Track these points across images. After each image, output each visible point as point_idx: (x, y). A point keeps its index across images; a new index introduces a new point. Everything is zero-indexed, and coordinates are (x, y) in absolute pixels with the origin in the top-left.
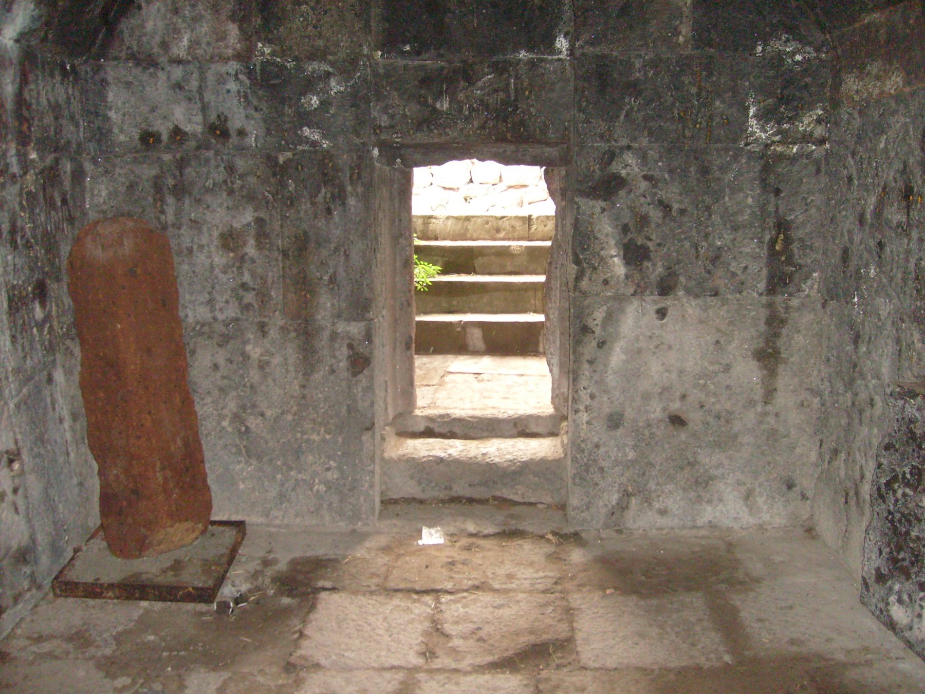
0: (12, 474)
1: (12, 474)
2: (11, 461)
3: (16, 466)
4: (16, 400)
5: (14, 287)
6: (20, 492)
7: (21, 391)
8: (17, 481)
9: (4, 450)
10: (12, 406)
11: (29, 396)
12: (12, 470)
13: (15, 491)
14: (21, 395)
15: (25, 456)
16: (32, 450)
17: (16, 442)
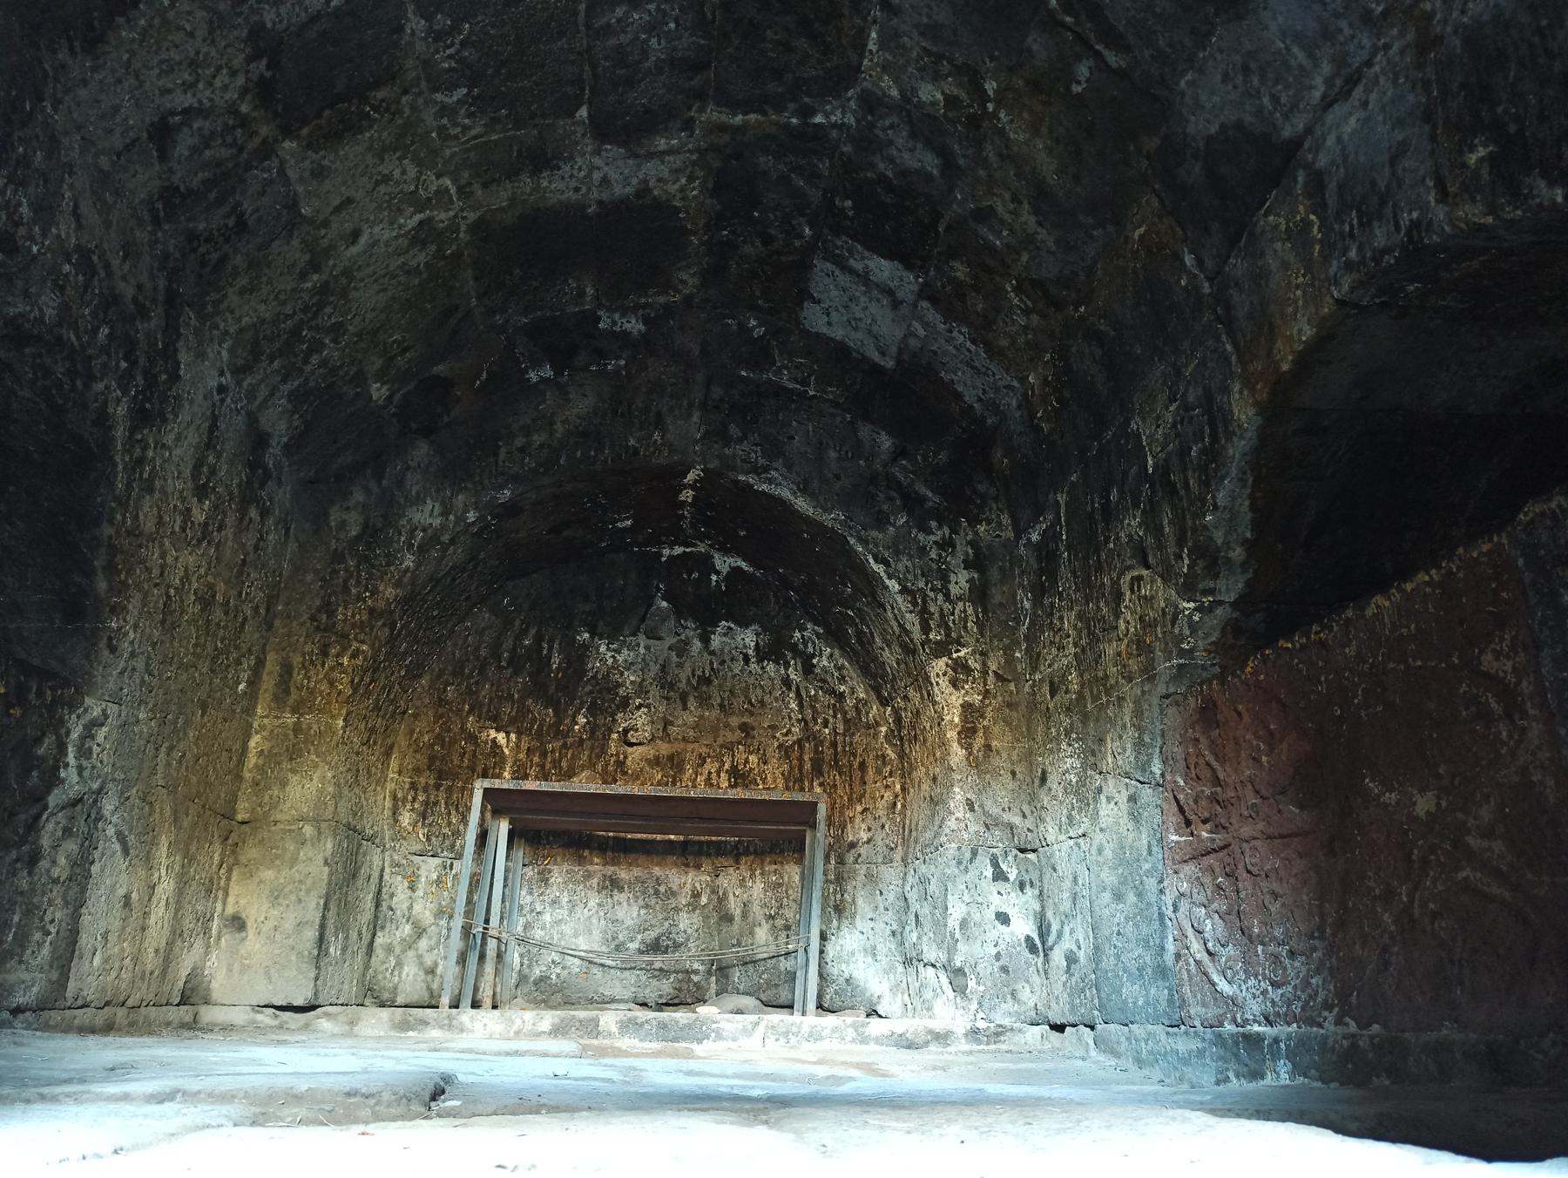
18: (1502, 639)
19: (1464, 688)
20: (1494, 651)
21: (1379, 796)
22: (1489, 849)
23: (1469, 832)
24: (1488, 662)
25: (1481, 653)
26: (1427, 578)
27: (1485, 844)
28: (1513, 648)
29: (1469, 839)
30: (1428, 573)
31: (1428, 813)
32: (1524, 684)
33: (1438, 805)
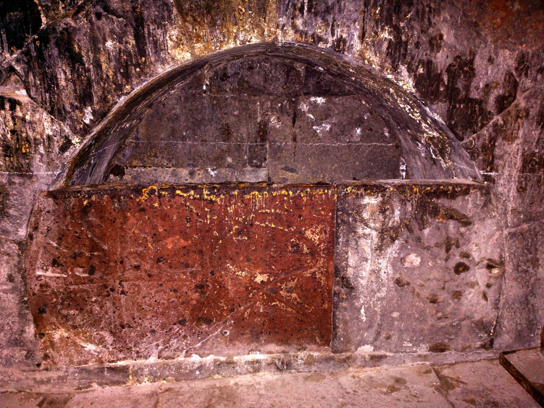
0: (490, 275)
1: (490, 275)
2: (490, 267)
3: (495, 271)
4: (513, 230)
5: (534, 154)
6: (492, 289)
7: (519, 225)
8: (492, 281)
9: (488, 257)
10: (506, 232)
11: (530, 230)
12: (491, 272)
13: (488, 286)
14: (519, 227)
15: (509, 268)
16: (519, 266)
17: (501, 257)
18: (316, 228)
19: (293, 240)
20: (311, 231)
21: (235, 272)
22: (290, 296)
23: (282, 290)
24: (308, 234)
25: (306, 230)
26: (287, 193)
27: (289, 294)
28: (321, 232)
29: (281, 292)
30: (287, 191)
31: (262, 282)
32: (322, 246)
33: (269, 279)
